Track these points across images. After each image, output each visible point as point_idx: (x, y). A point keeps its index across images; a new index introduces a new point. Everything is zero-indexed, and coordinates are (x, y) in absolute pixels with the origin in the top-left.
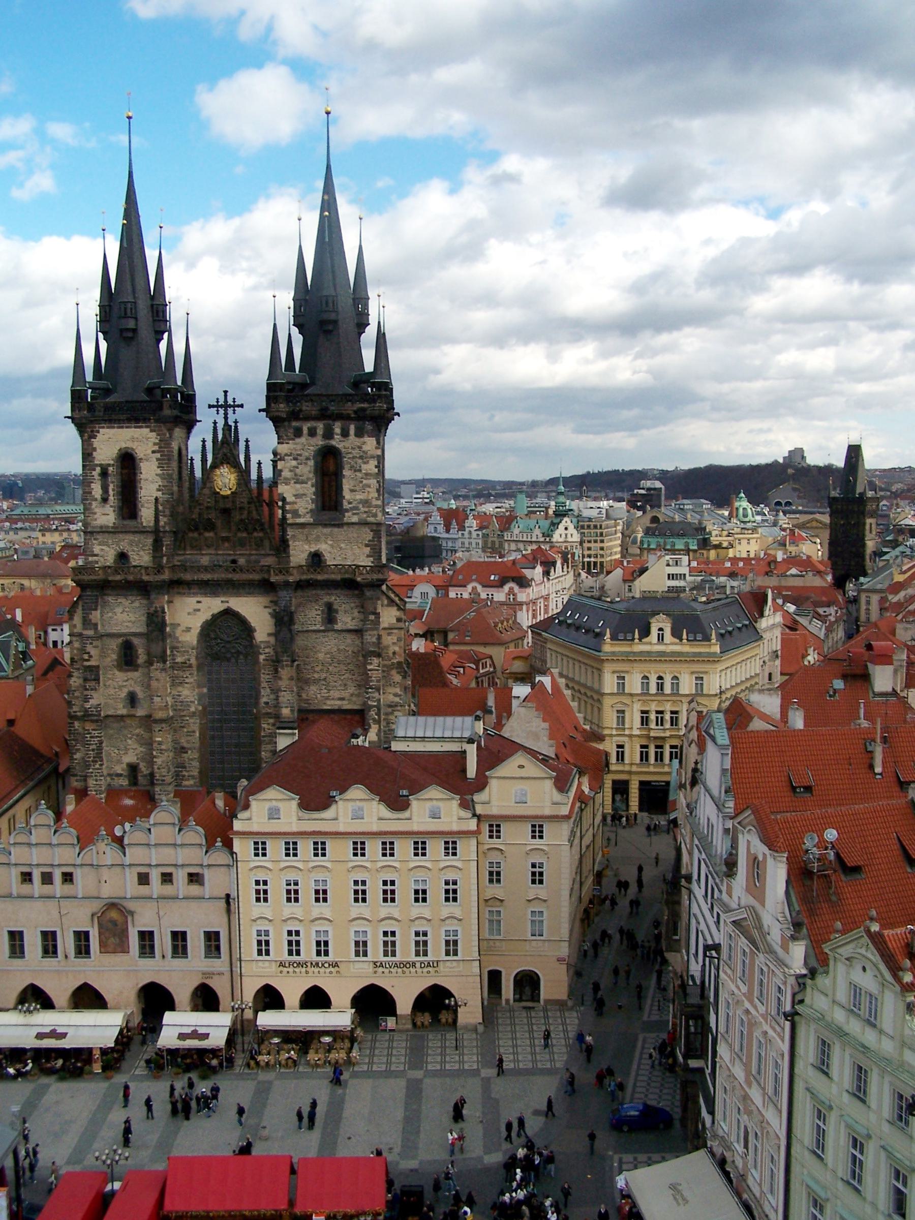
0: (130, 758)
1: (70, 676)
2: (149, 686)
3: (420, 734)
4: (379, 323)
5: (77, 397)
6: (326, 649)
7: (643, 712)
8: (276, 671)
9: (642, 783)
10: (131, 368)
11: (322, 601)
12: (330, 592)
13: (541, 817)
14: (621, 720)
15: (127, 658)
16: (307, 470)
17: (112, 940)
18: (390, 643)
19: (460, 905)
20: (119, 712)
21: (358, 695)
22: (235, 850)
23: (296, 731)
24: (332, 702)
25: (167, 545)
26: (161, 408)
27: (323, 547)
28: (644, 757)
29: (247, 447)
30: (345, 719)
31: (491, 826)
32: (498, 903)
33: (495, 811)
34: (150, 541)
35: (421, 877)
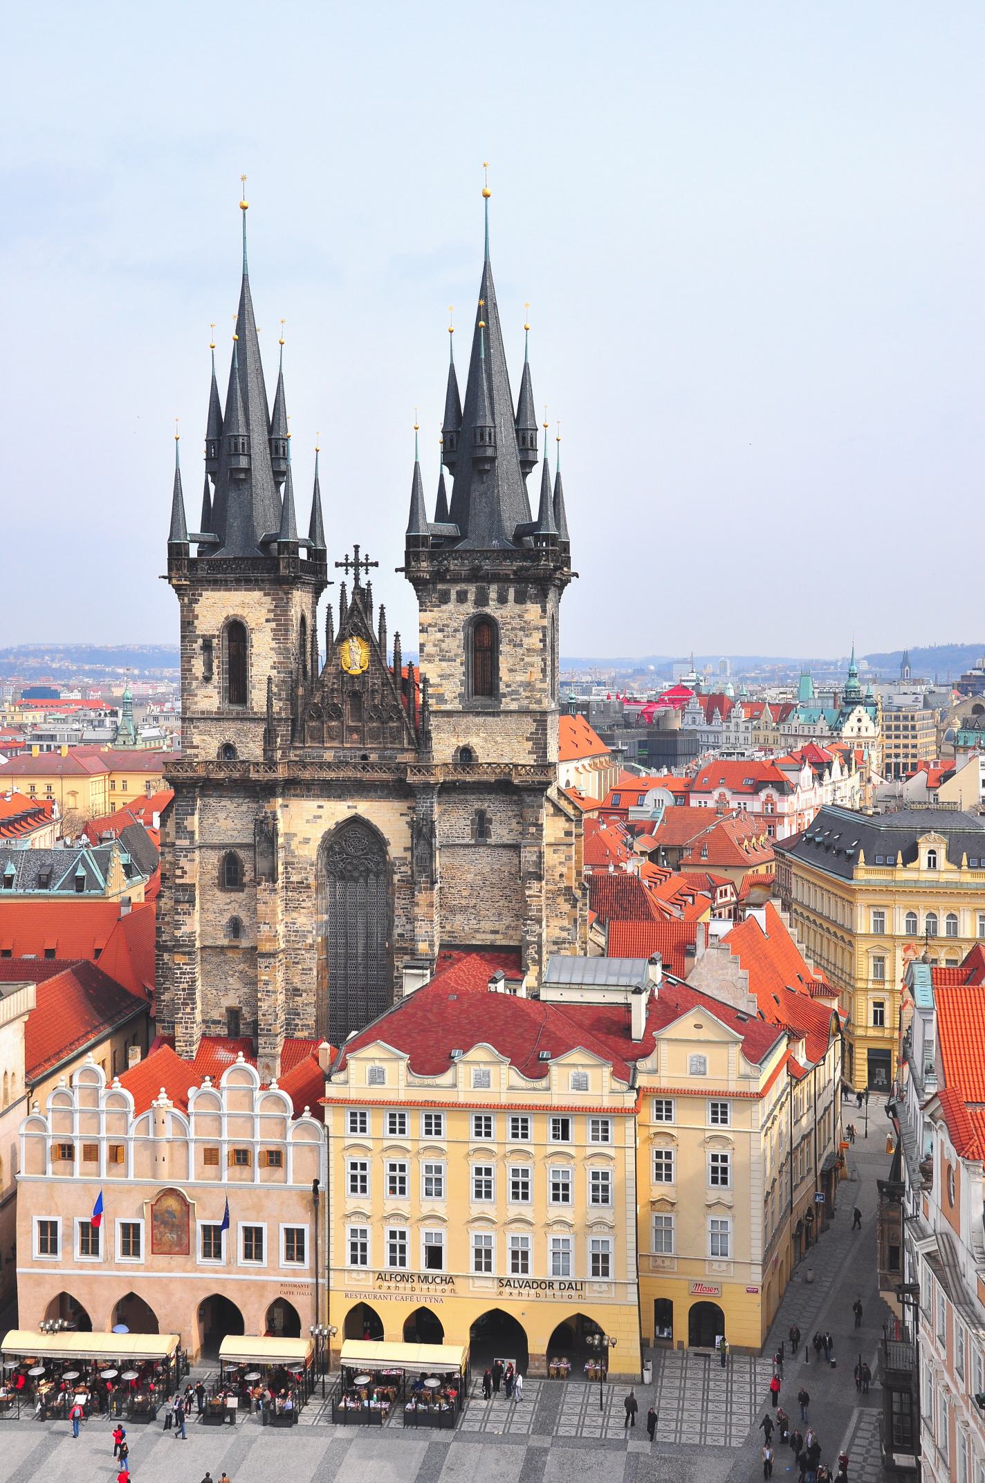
0: (231, 1001)
4: (545, 460)
5: (176, 552)
11: (471, 809)
13: (725, 1094)
15: (231, 875)
16: (456, 644)
17: (170, 1237)
19: (612, 1207)
20: (219, 943)
21: (516, 928)
22: (327, 1122)
23: (428, 972)
26: (278, 569)
27: (475, 741)
29: (382, 615)
30: (498, 957)
32: (669, 1208)
33: (665, 1084)
34: (260, 729)
35: (562, 1166)
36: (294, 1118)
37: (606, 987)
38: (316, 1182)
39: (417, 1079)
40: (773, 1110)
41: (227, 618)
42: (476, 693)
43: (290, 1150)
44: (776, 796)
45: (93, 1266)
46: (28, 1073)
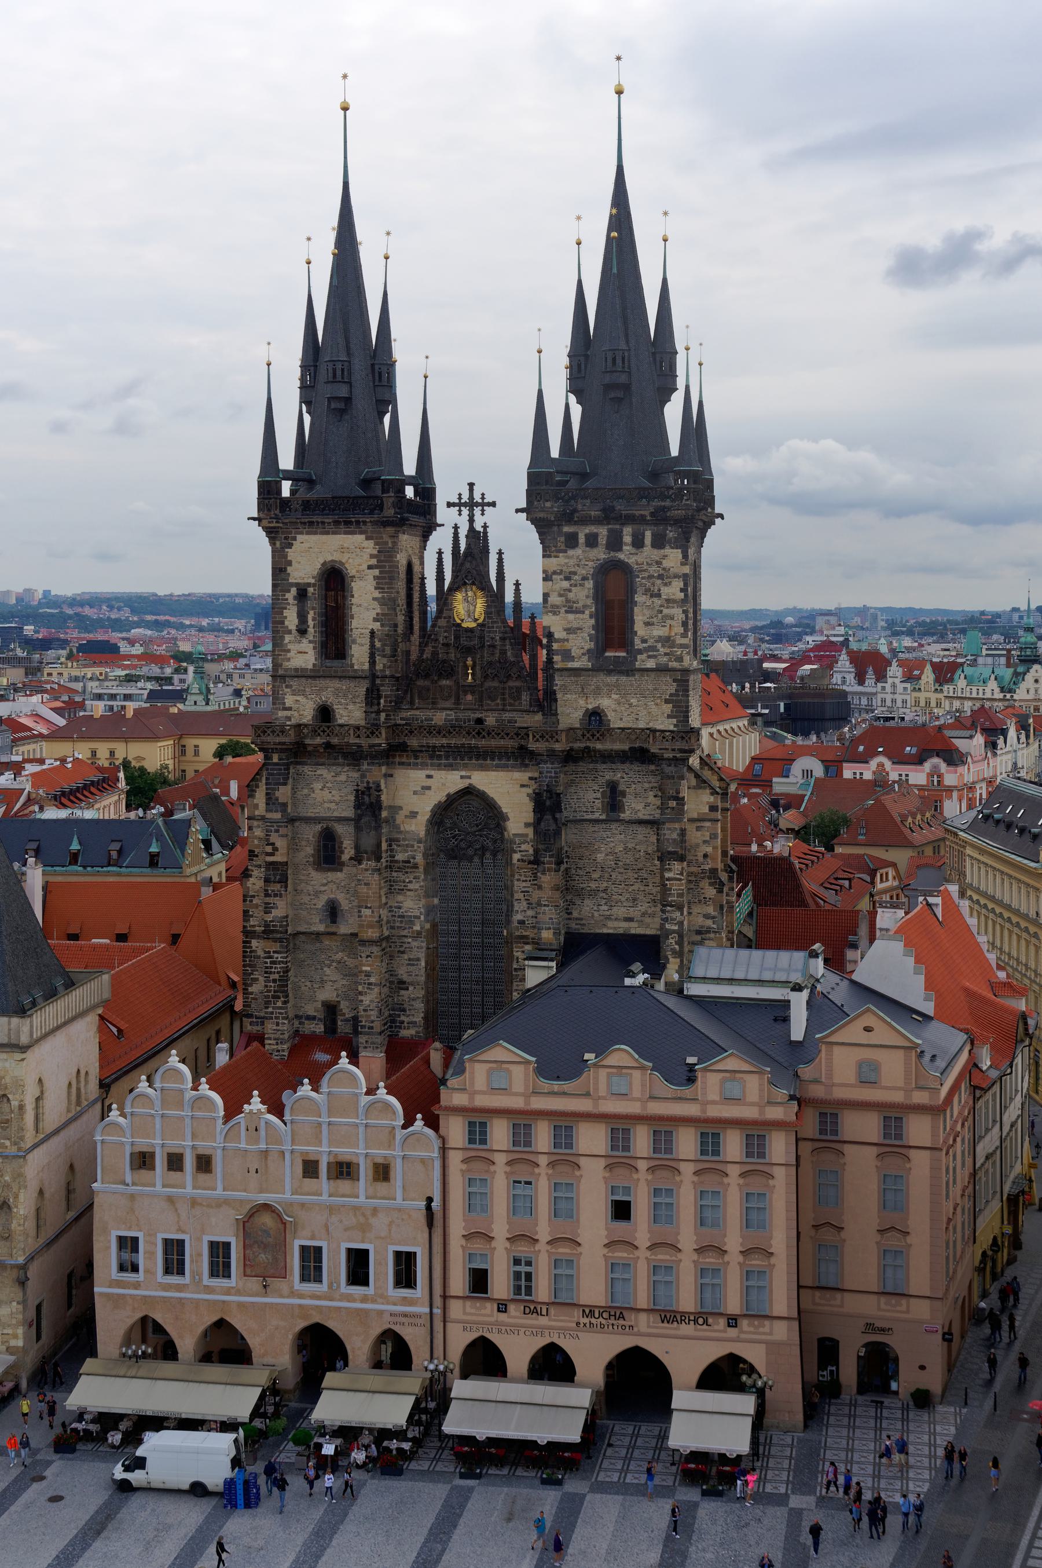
0: (327, 994)
6: (611, 846)
8: (536, 878)
10: (344, 445)
12: (614, 766)
18: (700, 842)
20: (314, 929)
22: (442, 1131)
23: (554, 964)
27: (606, 703)
34: (362, 691)
36: (404, 1127)
37: (760, 982)
38: (430, 1200)
39: (545, 1085)
45: (179, 1288)
46: (101, 1067)
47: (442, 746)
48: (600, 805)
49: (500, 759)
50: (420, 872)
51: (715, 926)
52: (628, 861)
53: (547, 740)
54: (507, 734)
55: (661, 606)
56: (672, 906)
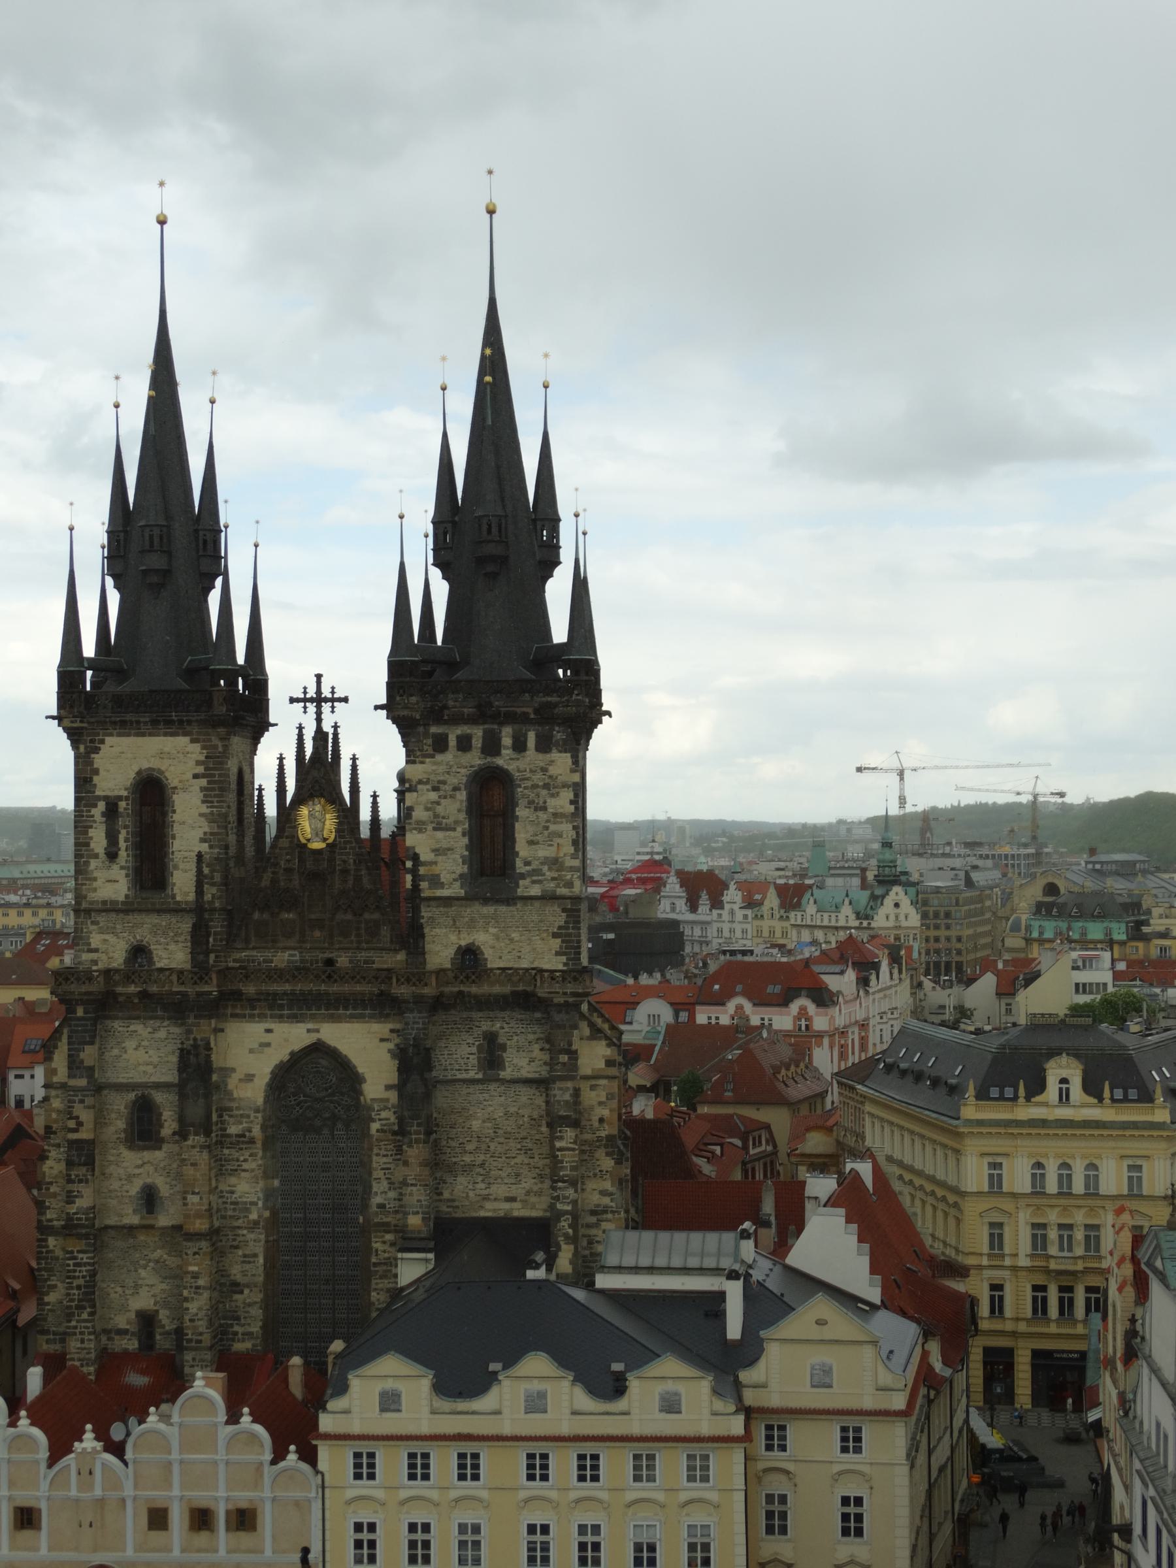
0: (143, 1301)
1: (43, 1157)
2: (179, 1175)
3: (645, 1262)
7: (1035, 1226)
8: (399, 1150)
9: (1036, 1354)
11: (478, 1032)
12: (491, 1014)
14: (996, 1240)
16: (455, 808)
18: (595, 1103)
20: (126, 1221)
21: (539, 1193)
22: (322, 1465)
24: (496, 1205)
25: (216, 933)
27: (483, 939)
28: (1040, 1306)
29: (354, 768)
31: (769, 1428)
33: (774, 1400)
34: (186, 925)
36: (274, 1462)
37: (685, 1270)
38: (306, 1551)
39: (446, 1405)
40: (915, 1434)
41: (139, 773)
42: (482, 873)
43: (268, 1507)
44: (811, 1008)
47: (285, 993)
48: (475, 1062)
49: (354, 1008)
50: (258, 1149)
51: (613, 1204)
52: (509, 1129)
53: (414, 984)
54: (364, 978)
55: (548, 821)
56: (564, 1182)
